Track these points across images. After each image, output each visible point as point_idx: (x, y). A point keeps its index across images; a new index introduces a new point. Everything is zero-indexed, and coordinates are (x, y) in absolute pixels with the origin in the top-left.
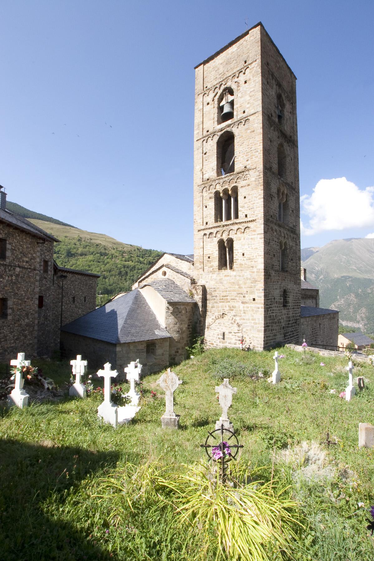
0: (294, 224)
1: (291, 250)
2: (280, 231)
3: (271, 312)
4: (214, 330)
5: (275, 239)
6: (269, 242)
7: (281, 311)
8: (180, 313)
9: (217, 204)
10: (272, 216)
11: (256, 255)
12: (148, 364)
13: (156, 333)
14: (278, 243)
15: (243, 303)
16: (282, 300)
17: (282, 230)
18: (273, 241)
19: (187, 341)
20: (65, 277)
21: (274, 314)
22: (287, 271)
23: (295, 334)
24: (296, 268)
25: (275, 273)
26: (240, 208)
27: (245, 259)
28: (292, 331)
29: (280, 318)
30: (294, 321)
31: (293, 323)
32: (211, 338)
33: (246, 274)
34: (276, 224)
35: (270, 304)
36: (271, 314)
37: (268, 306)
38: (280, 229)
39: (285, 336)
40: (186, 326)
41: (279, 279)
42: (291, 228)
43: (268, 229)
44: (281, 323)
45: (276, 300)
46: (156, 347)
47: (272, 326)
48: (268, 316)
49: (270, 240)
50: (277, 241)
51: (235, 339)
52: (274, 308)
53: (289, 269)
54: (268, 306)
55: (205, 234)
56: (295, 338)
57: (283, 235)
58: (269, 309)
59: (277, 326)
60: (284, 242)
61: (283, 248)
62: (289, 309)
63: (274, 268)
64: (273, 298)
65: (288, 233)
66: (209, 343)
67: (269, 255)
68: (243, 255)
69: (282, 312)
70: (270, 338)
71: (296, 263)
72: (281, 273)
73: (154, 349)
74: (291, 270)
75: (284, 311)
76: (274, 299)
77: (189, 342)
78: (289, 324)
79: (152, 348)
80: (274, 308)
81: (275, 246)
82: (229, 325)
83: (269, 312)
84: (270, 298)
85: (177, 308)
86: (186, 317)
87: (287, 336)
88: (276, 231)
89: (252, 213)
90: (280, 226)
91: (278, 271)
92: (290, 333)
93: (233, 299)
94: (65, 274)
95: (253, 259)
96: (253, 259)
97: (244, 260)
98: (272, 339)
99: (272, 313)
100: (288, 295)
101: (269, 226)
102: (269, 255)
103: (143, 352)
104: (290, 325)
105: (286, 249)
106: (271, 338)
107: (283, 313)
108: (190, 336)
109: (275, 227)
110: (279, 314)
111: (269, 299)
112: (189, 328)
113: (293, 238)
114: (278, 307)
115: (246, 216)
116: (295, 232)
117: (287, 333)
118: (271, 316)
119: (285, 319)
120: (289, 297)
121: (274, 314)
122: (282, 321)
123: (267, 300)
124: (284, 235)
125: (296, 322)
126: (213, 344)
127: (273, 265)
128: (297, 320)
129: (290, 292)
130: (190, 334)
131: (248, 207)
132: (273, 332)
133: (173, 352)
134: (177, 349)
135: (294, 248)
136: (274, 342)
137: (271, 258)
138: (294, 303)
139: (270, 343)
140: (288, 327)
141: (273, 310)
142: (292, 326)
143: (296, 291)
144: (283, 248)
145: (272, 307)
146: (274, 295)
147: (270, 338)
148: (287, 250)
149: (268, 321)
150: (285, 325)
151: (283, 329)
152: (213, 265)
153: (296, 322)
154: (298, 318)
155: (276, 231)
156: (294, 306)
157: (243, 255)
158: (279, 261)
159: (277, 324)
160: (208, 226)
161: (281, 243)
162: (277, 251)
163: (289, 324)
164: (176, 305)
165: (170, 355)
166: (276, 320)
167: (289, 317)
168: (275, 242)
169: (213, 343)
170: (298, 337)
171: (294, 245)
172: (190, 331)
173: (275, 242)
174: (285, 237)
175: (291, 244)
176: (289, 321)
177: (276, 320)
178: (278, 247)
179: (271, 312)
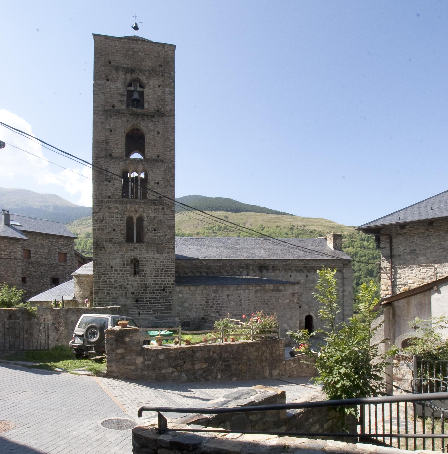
21: (113, 280)
36: (106, 280)
37: (99, 273)
44: (125, 288)
45: (113, 268)
49: (103, 217)
58: (103, 276)
62: (144, 276)
71: (165, 232)
81: (115, 222)
83: (102, 279)
84: (102, 266)
100: (142, 263)
110: (122, 281)
111: (102, 267)
118: (106, 282)
119: (135, 284)
129: (147, 261)
138: (156, 271)
140: (142, 293)
141: (109, 277)
142: (154, 293)
145: (108, 274)
146: (111, 264)
153: (164, 290)
159: (118, 289)
166: (115, 285)
168: (116, 217)
170: (171, 305)
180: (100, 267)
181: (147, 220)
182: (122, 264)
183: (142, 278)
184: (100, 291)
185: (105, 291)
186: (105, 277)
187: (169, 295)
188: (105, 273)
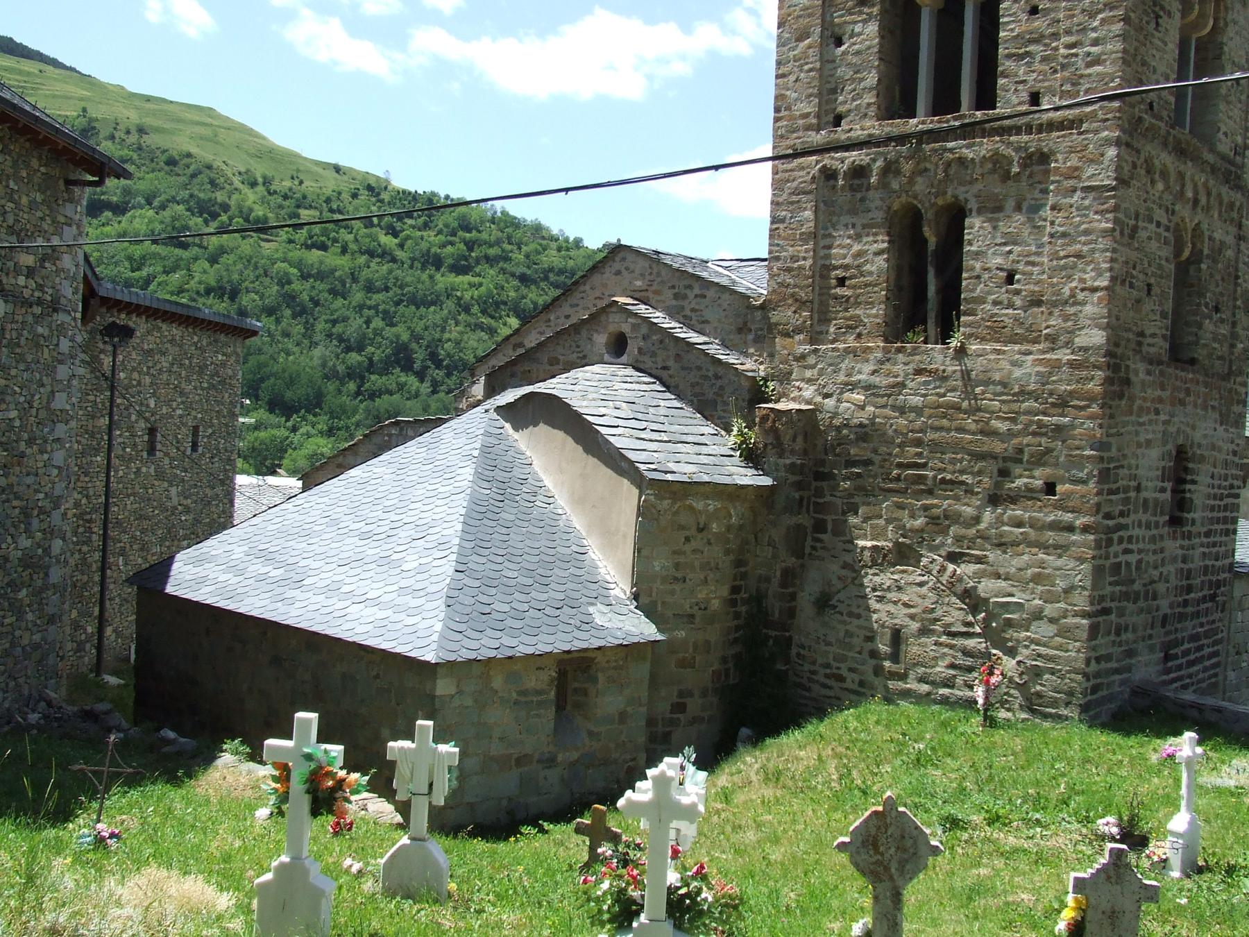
0: (1239, 139)
1: (1215, 261)
2: (1181, 176)
3: (1120, 548)
4: (851, 614)
5: (1160, 215)
6: (1135, 229)
7: (1158, 545)
8: (701, 530)
9: (891, 32)
10: (1151, 105)
11: (1074, 284)
12: (560, 758)
13: (599, 620)
14: (1167, 229)
15: (994, 500)
16: (1168, 496)
17: (1189, 169)
18: (1151, 221)
19: (724, 660)
20: (127, 332)
21: (1133, 558)
22: (1193, 362)
23: (1207, 651)
24: (1233, 346)
25: (1149, 373)
26: (1005, 65)
27: (1018, 301)
28: (1194, 638)
29: (1155, 574)
30: (1205, 592)
31: (1204, 598)
32: (834, 649)
33: (1018, 373)
34: (1165, 144)
35: (1122, 514)
36: (1121, 558)
37: (1111, 523)
38: (1182, 168)
39: (1167, 658)
40: (725, 591)
41: (1160, 400)
42: (1224, 158)
43: (1134, 166)
46: (594, 680)
47: (1121, 613)
48: (1108, 563)
49: (1137, 218)
50: (1164, 221)
51: (947, 661)
52: (1136, 532)
53: (1200, 354)
54: (1111, 523)
55: (829, 174)
56: (1205, 669)
57: (1190, 194)
58: (1115, 537)
59: (1141, 611)
60: (1190, 226)
61: (1186, 253)
63: (1145, 349)
64: (1133, 484)
65: (1212, 182)
66: (822, 671)
67: (1131, 286)
68: (1010, 279)
69: (1162, 550)
70: (1109, 665)
71: (1234, 324)
72: (1170, 370)
73: (585, 693)
74: (1210, 355)
75: (1173, 546)
76: (1138, 489)
77: (731, 665)
78: (1186, 603)
79: (576, 685)
80: (1136, 532)
81: (1154, 245)
82: (923, 597)
84: (1121, 483)
85: (691, 508)
86: (727, 552)
87: (1176, 657)
88: (1164, 175)
89: (1067, 87)
90: (1181, 152)
91: (1160, 363)
92: (1186, 646)
93: (951, 482)
94: (122, 319)
95: (1054, 304)
96: (1054, 304)
97: (1011, 305)
98: (1117, 671)
99: (1126, 551)
100: (1192, 472)
101: (1138, 151)
102: (1131, 286)
103: (540, 704)
104: (1190, 609)
105: (1196, 257)
106: (1114, 665)
107: (1167, 554)
108: (736, 641)
109: (1165, 159)
110: (1151, 558)
112: (733, 603)
113: (1231, 205)
114: (1148, 527)
115: (1035, 99)
116: (1239, 177)
117: (1177, 643)
118: (1120, 563)
120: (1194, 482)
121: (1133, 558)
122: (1161, 588)
123: (1111, 492)
124: (1196, 192)
125: (1213, 598)
126: (841, 679)
127: (1142, 334)
128: (1218, 584)
129: (1202, 459)
130: (737, 628)
131: (1044, 59)
132: (1124, 637)
133: (663, 708)
134: (681, 694)
135: (1230, 253)
136: (1123, 683)
137: (1138, 301)
138: (1212, 509)
139: (1109, 685)
140: (1182, 617)
141: (1130, 539)
143: (1221, 457)
144: (1186, 253)
146: (1140, 472)
147: (1109, 665)
148: (1201, 261)
149: (1109, 589)
150: (1171, 606)
151: (1163, 626)
152: (857, 319)
154: (1223, 576)
155: (1164, 175)
156: (1212, 521)
157: (1010, 279)
158: (1164, 315)
159: (1141, 603)
160: (841, 134)
161: (1178, 231)
162: (1160, 267)
163: (1186, 603)
164: (686, 496)
165: (651, 722)
166: (1137, 586)
167: (1189, 571)
168: (1158, 224)
169: (844, 672)
171: (1230, 240)
172: (737, 616)
173: (1158, 224)
174: (1196, 202)
175: (1217, 236)
176: (1189, 589)
177: (1137, 586)
178: (1166, 252)
179: (1120, 548)
180: (1114, 486)
181: (1208, 256)
182: (1159, 473)
183: (1186, 543)
184: (1100, 619)
185: (1113, 617)
186: (1121, 541)
187: (1220, 620)
188: (1122, 520)
